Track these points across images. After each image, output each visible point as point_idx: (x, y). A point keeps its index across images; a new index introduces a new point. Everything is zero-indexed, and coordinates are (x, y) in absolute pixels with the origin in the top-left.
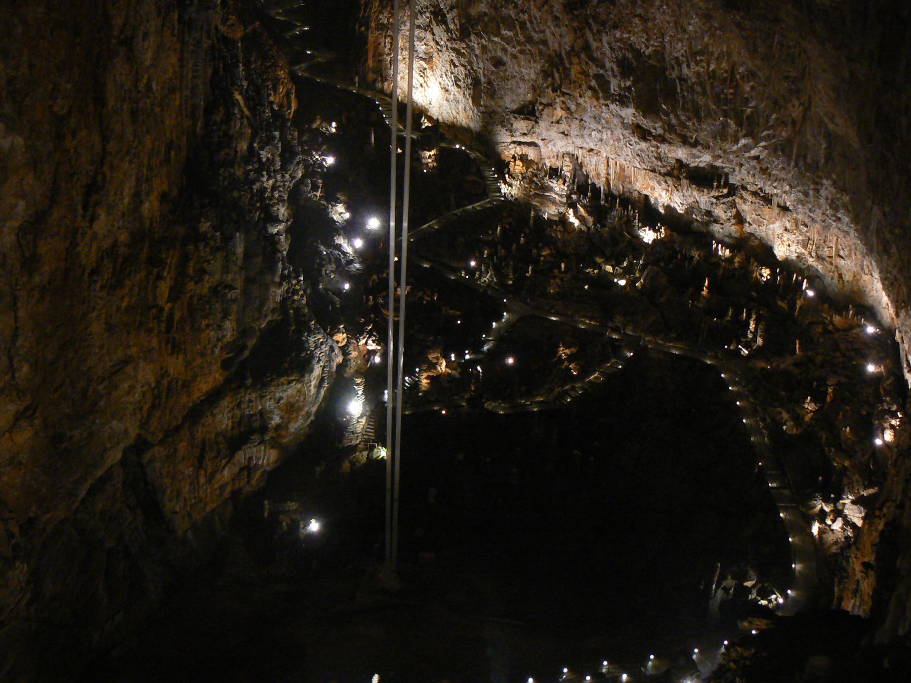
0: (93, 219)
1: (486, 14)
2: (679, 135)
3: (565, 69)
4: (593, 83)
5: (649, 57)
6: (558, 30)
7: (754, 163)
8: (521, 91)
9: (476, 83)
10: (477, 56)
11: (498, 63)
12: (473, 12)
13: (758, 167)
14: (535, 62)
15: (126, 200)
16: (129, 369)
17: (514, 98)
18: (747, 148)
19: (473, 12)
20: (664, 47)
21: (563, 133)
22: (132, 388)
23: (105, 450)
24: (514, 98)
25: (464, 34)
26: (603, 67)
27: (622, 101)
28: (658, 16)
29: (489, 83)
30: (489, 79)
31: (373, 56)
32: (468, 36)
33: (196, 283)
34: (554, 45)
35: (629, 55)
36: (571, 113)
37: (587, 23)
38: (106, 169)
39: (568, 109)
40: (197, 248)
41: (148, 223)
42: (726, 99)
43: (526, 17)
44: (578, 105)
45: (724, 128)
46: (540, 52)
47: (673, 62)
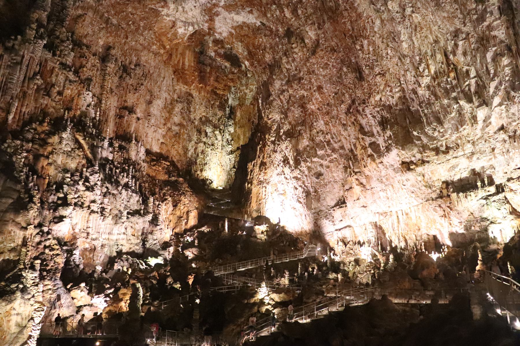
1: (308, 146)
2: (433, 149)
4: (370, 151)
5: (397, 105)
7: (502, 136)
8: (336, 190)
9: (308, 194)
10: (306, 176)
12: (301, 147)
13: (507, 138)
17: (332, 197)
18: (487, 120)
21: (364, 206)
24: (332, 197)
25: (297, 163)
29: (316, 191)
30: (315, 189)
31: (256, 202)
32: (300, 164)
36: (364, 186)
39: (362, 184)
42: (453, 87)
43: (329, 137)
44: (367, 177)
45: (460, 114)
46: (341, 156)
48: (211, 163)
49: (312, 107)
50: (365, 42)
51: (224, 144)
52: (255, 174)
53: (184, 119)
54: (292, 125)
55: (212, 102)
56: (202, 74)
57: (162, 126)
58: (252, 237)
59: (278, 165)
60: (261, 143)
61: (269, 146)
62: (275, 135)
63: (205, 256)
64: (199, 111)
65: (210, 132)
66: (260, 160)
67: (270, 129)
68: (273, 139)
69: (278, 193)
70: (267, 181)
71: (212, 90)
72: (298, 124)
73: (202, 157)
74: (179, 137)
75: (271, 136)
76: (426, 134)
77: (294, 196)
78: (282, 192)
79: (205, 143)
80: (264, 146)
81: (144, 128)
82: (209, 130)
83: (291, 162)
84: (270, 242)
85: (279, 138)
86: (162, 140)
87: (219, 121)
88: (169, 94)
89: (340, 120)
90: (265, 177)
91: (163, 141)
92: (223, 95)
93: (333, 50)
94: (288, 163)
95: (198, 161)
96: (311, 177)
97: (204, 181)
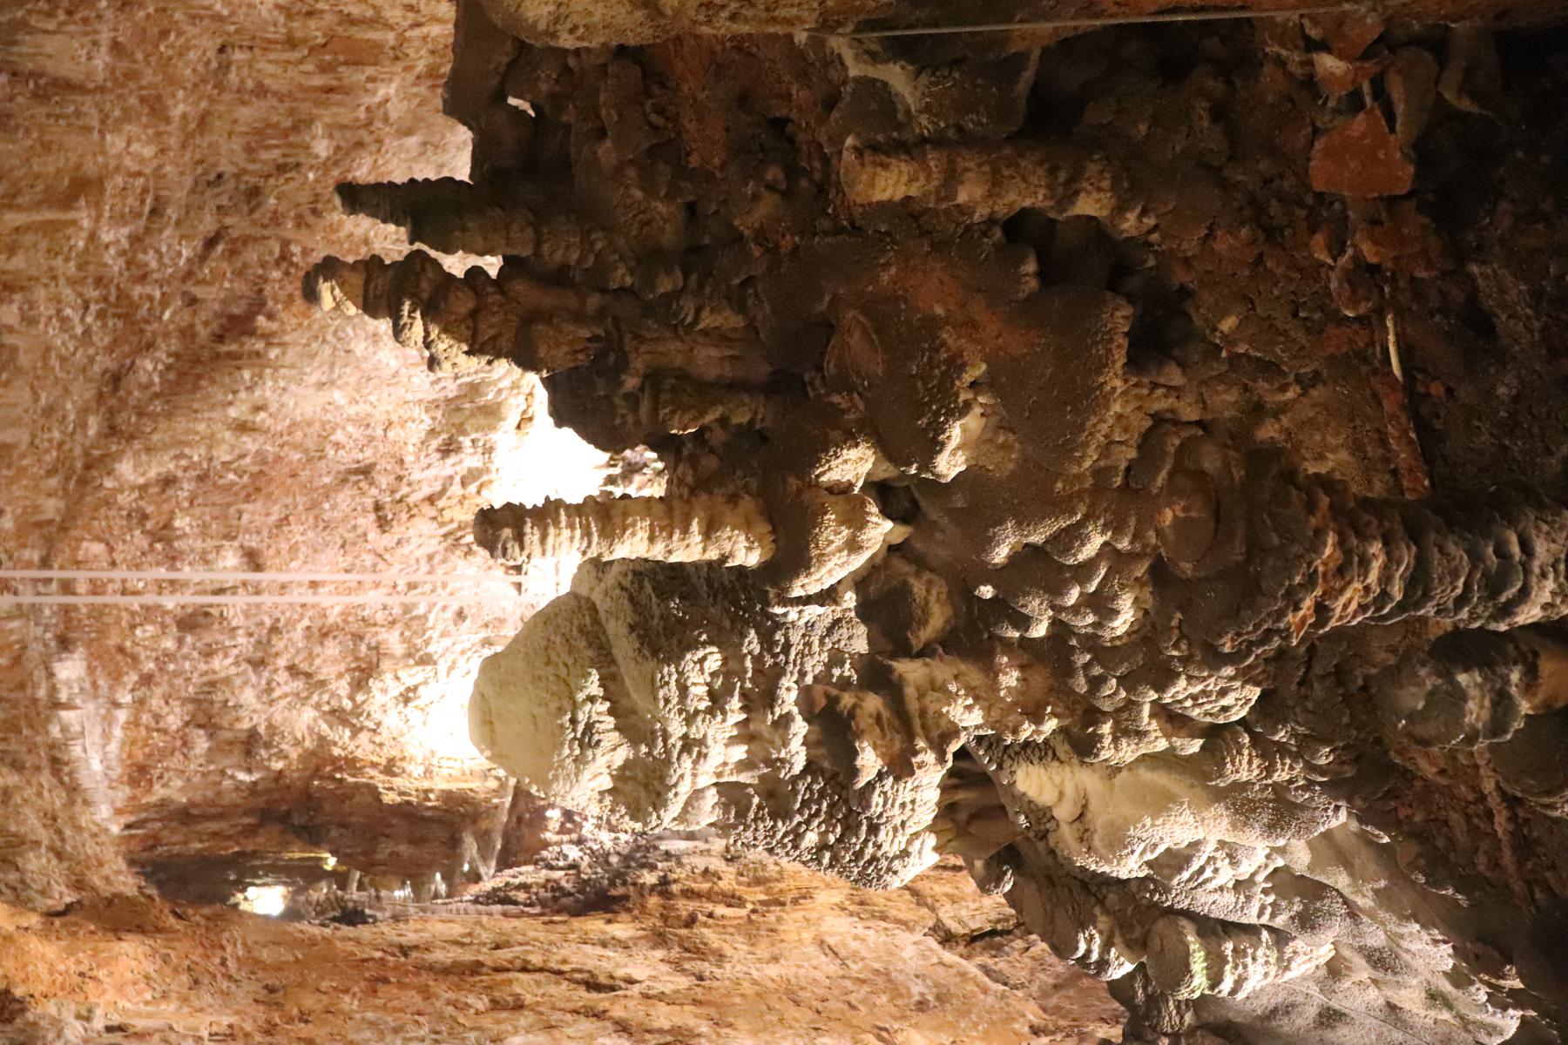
0: (631, 981)
3: (460, 528)
4: (472, 488)
5: (434, 419)
6: (413, 540)
11: (460, 615)
14: (455, 569)
15: (611, 954)
16: (831, 941)
20: (420, 401)
22: (856, 938)
23: (941, 963)
26: (451, 478)
27: (489, 450)
28: (383, 408)
32: (429, 656)
33: (720, 878)
34: (433, 545)
35: (435, 443)
37: (400, 501)
38: (566, 968)
40: (675, 881)
41: (641, 933)
46: (444, 561)
47: (437, 387)
50: (339, 436)
54: (348, 670)
60: (338, 776)
67: (322, 739)
76: (499, 379)
89: (386, 549)
93: (284, 521)
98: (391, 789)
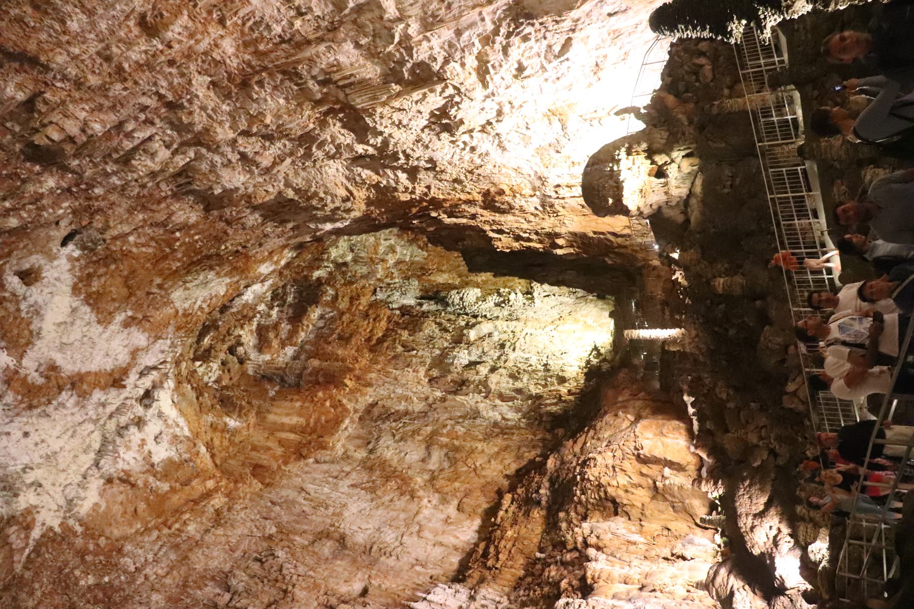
1: (357, 45)
10: (459, 33)
12: (371, 71)
19: (371, 71)
25: (425, 77)
48: (548, 352)
49: (230, 50)
51: (506, 313)
52: (525, 226)
53: (415, 432)
55: (400, 349)
56: (321, 379)
57: (413, 507)
58: (687, 221)
59: (473, 149)
60: (434, 214)
61: (428, 187)
62: (388, 171)
63: (773, 453)
64: (410, 386)
65: (469, 354)
66: (480, 211)
68: (403, 176)
69: (563, 141)
70: (538, 183)
71: (371, 350)
72: (304, 93)
73: (525, 378)
74: (457, 449)
75: (397, 182)
77: (551, 73)
78: (557, 125)
79: (493, 370)
80: (436, 204)
81: (397, 574)
82: (463, 357)
83: (435, 101)
84: (701, 128)
85: (384, 158)
86: (451, 510)
87: (446, 330)
88: (348, 474)
90: (527, 191)
91: (455, 502)
92: (389, 320)
94: (443, 112)
95: (534, 390)
96: (455, 12)
97: (592, 372)
98: (500, 232)
